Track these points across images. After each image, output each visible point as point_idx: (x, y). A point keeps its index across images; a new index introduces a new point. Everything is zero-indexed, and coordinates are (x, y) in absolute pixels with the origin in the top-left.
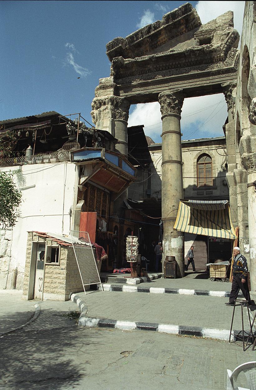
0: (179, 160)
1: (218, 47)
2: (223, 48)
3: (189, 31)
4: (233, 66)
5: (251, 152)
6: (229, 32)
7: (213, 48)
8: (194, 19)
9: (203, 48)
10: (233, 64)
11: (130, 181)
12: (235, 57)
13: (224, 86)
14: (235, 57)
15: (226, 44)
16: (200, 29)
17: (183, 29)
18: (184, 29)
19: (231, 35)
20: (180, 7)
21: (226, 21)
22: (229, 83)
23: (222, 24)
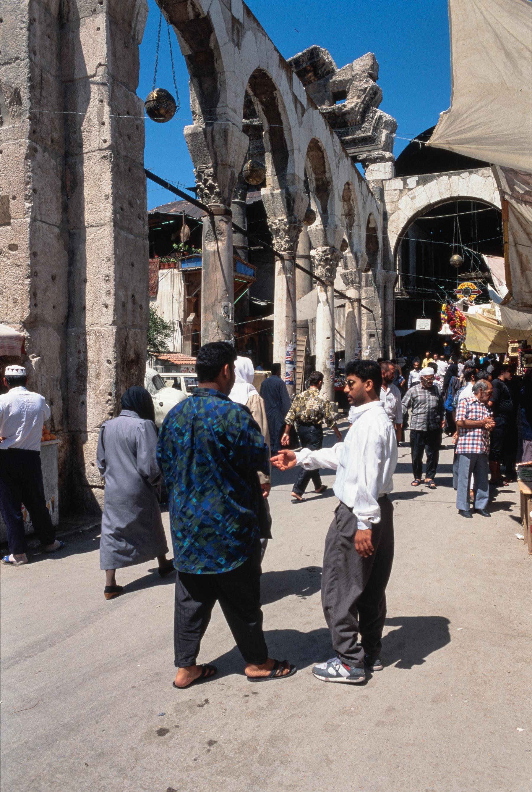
0: (307, 254)
1: (352, 109)
2: (359, 109)
3: (319, 79)
4: (370, 134)
5: (348, 269)
6: (366, 86)
7: (346, 109)
8: (324, 64)
9: (334, 110)
10: (371, 131)
11: (248, 283)
12: (374, 122)
13: (360, 158)
14: (374, 122)
15: (362, 103)
16: (334, 78)
17: (311, 77)
18: (313, 78)
19: (369, 91)
20: (304, 51)
21: (364, 68)
22: (365, 155)
23: (359, 72)
